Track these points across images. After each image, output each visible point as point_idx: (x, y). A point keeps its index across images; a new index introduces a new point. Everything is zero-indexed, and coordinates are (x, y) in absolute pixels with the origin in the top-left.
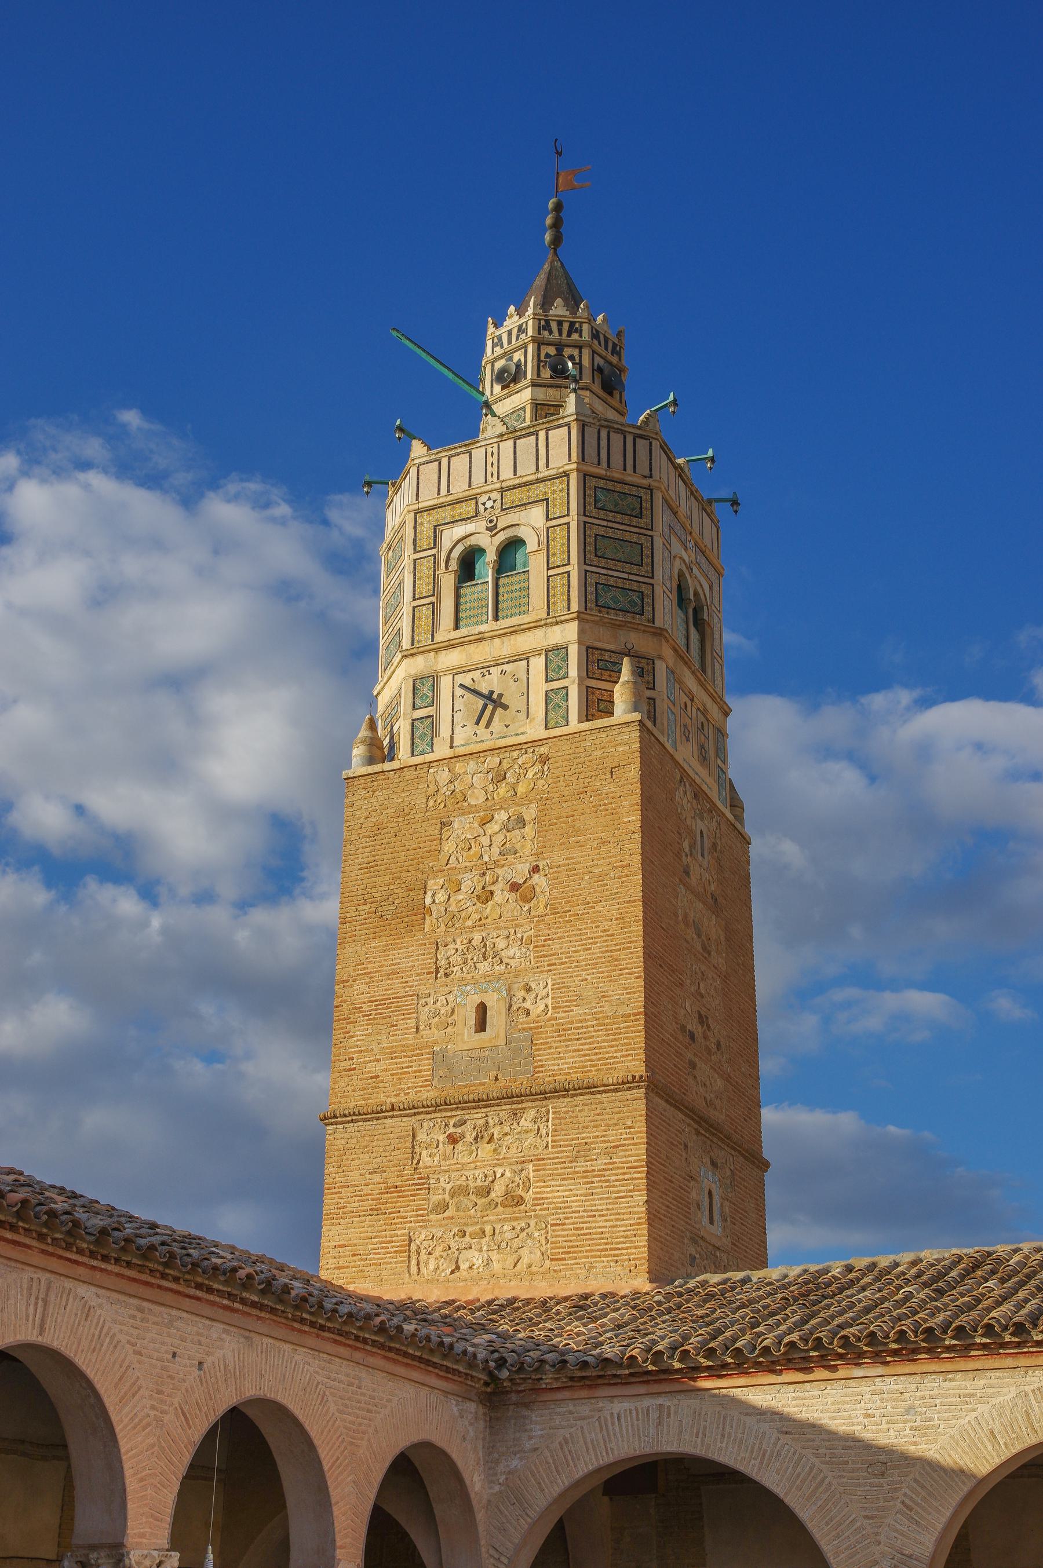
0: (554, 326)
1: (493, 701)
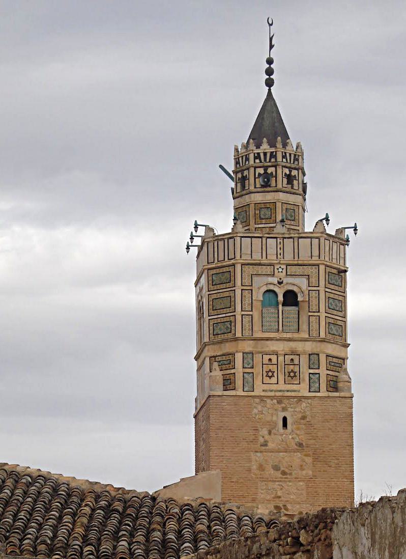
0: (288, 155)
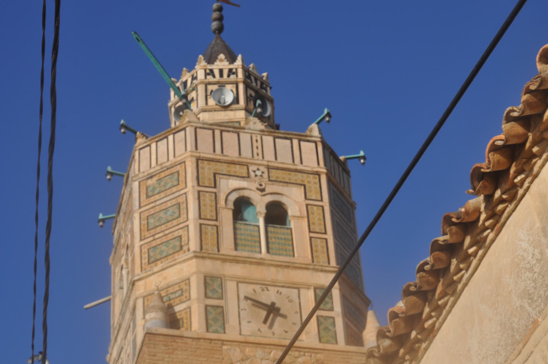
0: (253, 78)
1: (272, 310)
